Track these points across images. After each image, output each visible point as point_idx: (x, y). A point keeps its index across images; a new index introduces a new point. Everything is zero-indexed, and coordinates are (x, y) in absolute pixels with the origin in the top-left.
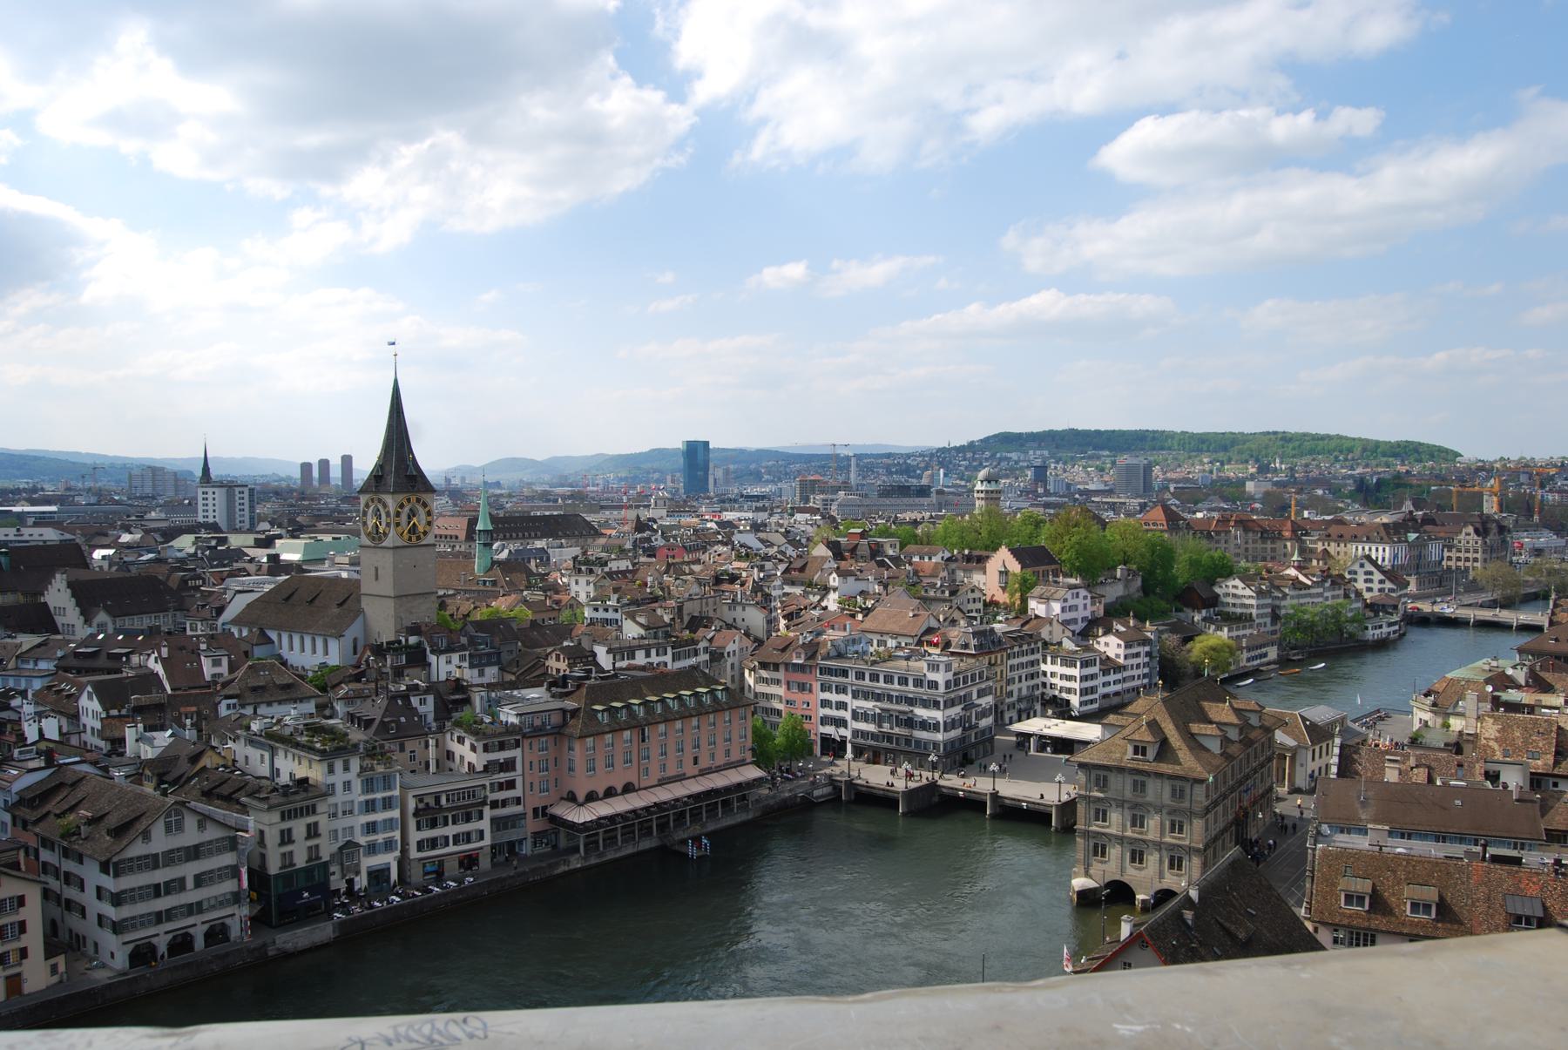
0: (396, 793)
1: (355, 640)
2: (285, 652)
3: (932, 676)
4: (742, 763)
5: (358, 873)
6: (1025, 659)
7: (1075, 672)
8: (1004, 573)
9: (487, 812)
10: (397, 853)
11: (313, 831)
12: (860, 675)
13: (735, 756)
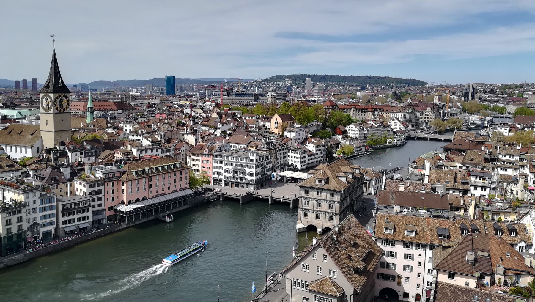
0: (55, 204)
1: (38, 148)
2: (8, 153)
3: (251, 158)
4: (186, 188)
5: (38, 234)
6: (282, 152)
7: (299, 156)
8: (277, 123)
9: (91, 209)
10: (55, 226)
11: (20, 220)
12: (227, 157)
13: (183, 186)
